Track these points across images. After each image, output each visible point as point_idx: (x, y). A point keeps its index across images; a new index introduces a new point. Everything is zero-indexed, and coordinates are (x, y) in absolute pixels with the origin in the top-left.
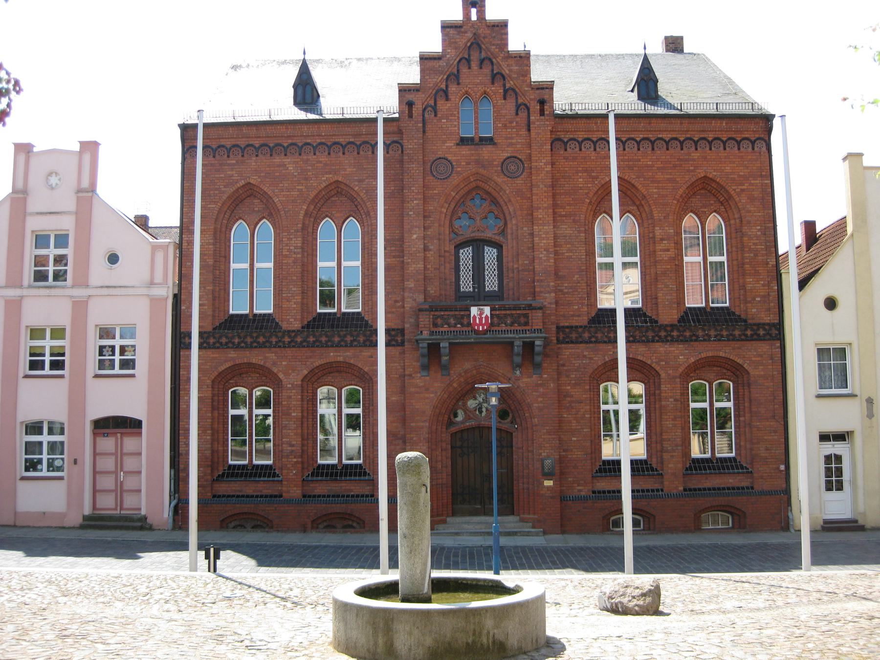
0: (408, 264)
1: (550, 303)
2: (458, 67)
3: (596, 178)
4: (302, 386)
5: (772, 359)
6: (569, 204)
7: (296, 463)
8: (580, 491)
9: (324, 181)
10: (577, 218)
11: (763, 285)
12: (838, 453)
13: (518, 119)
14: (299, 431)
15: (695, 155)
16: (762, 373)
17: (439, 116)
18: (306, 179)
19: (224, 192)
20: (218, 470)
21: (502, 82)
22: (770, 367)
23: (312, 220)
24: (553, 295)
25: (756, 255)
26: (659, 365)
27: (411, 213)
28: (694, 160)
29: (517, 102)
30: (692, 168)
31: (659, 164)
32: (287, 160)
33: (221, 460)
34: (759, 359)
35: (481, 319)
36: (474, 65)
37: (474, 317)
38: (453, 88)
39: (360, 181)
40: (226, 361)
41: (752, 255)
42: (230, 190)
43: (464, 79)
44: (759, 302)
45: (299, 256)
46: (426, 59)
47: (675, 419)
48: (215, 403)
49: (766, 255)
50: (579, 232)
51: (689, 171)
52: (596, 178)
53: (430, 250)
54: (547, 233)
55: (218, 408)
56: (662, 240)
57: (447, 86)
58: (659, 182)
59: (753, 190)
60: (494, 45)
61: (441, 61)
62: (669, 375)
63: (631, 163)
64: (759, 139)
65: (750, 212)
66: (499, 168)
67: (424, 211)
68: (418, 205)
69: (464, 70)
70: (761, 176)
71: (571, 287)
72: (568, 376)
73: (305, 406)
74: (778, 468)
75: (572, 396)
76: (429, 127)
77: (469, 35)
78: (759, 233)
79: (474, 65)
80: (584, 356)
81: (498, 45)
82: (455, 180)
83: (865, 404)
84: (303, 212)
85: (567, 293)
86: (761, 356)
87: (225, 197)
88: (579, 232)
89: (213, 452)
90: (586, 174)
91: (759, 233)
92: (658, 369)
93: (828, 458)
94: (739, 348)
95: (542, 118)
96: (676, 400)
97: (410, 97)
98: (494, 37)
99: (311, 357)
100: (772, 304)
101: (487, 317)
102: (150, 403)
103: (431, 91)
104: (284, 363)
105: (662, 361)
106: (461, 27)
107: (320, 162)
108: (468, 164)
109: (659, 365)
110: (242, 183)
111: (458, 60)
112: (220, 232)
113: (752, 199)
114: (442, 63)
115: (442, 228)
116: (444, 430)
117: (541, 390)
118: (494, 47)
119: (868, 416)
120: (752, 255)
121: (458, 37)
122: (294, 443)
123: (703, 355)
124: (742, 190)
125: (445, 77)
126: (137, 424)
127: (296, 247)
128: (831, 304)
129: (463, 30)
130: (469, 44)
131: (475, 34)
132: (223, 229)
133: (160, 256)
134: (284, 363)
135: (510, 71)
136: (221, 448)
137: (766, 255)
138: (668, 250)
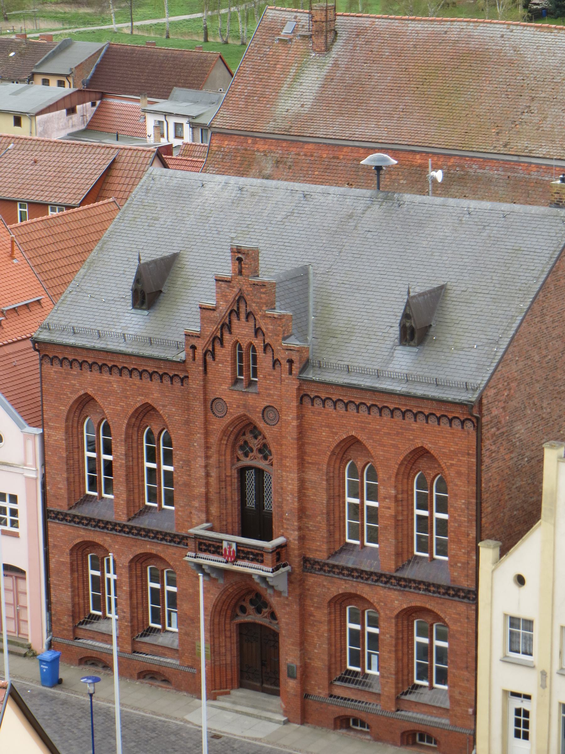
0: (194, 486)
1: (294, 540)
2: (230, 318)
3: (336, 434)
4: (130, 566)
5: (468, 618)
6: (316, 455)
7: (127, 626)
8: (320, 693)
9: (139, 401)
10: (320, 467)
11: (464, 553)
12: (527, 709)
13: (275, 373)
14: (129, 602)
15: (415, 426)
16: (459, 629)
17: (217, 360)
18: (126, 397)
19: (69, 398)
20: (79, 618)
21: (262, 337)
22: (466, 625)
23: (136, 429)
24: (296, 533)
25: (460, 526)
26: (379, 605)
27: (195, 444)
28: (414, 430)
29: (273, 357)
30: (412, 437)
31: (385, 430)
32: (112, 378)
33: (82, 610)
34: (458, 616)
35: (230, 552)
36: (243, 316)
37: (225, 550)
38: (227, 336)
39: (164, 406)
40: (78, 537)
41: (456, 525)
42: (75, 397)
43: (235, 330)
44: (460, 567)
45: (124, 462)
46: (204, 308)
47: (390, 652)
48: (75, 567)
49: (468, 527)
50: (322, 479)
51: (409, 440)
52: (336, 434)
53: (211, 476)
54: (292, 480)
55: (78, 570)
56: (385, 498)
57: (222, 335)
58: (384, 446)
59: (461, 466)
60: (254, 302)
61: (215, 312)
62: (386, 614)
63: (363, 425)
64: (467, 419)
65: (457, 485)
66: (261, 415)
67: (206, 442)
68: (200, 438)
69: (235, 320)
70: (469, 454)
71: (315, 526)
72: (312, 599)
73: (134, 582)
74: (467, 711)
75: (314, 616)
76: (209, 368)
77: (236, 290)
78: (463, 506)
79: (243, 316)
80: (324, 586)
81: (258, 303)
82: (228, 419)
83: (540, 675)
84: (125, 425)
85: (312, 531)
86: (459, 614)
87: (71, 402)
88: (322, 479)
89: (73, 606)
90: (327, 429)
91: (463, 506)
92: (378, 608)
93: (518, 712)
94: (442, 604)
95: (291, 376)
96: (391, 637)
97: (194, 342)
98: (255, 295)
99: (133, 546)
100: (470, 572)
101: (233, 551)
102: (30, 560)
103: (208, 338)
104: (116, 547)
105: (382, 602)
106: (229, 282)
107: (135, 384)
108: (238, 407)
109: (379, 605)
110: (82, 392)
111: (229, 311)
112: (72, 427)
113: (459, 474)
114: (216, 314)
115: (223, 457)
116: (228, 621)
117: (287, 609)
118: (254, 305)
119: (541, 686)
120: (456, 525)
121: (228, 290)
122: (125, 610)
123: (413, 604)
124: (452, 465)
125: (219, 326)
126: (23, 572)
127: (121, 454)
128: (520, 580)
129: (231, 284)
130: (237, 298)
131: (240, 290)
132: (75, 425)
133: (30, 444)
134: (116, 547)
135: (267, 329)
136: (81, 601)
137: (468, 527)
138: (389, 508)
